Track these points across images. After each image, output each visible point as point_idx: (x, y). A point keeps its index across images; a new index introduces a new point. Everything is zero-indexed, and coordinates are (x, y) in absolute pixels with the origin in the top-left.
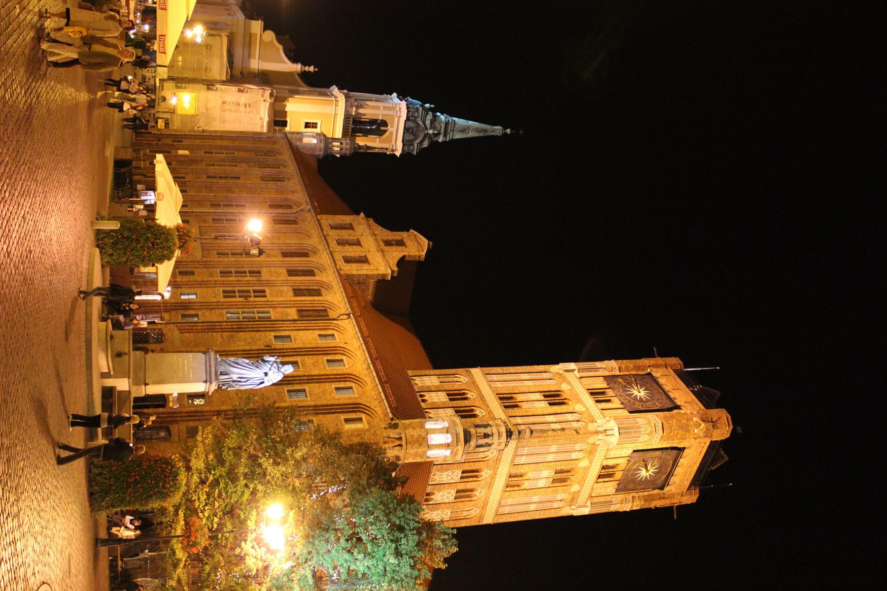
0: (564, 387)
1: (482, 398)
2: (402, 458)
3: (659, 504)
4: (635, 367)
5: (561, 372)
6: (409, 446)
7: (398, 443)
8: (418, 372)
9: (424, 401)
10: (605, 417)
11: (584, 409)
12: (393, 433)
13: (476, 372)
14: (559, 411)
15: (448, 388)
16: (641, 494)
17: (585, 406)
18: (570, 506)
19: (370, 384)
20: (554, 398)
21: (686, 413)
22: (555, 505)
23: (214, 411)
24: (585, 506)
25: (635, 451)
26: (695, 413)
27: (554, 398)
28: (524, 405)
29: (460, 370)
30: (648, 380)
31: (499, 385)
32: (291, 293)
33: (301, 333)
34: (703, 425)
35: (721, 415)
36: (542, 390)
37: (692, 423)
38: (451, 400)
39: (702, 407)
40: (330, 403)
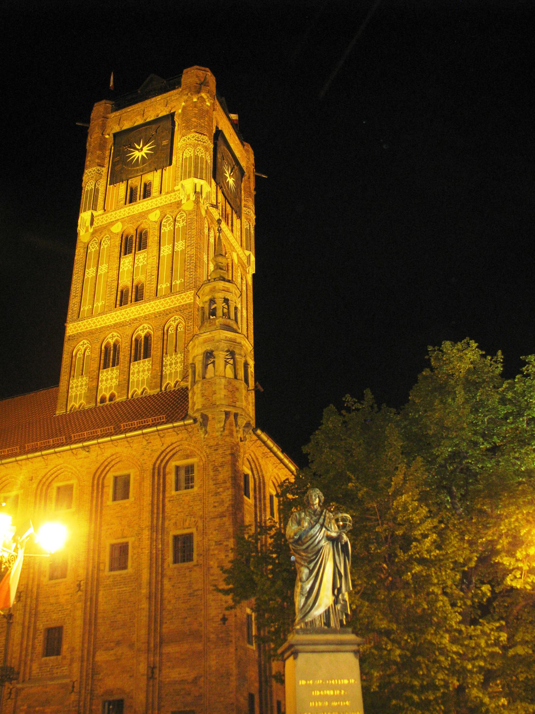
0: (117, 229)
1: (117, 326)
2: (248, 419)
3: (252, 186)
4: (100, 149)
5: (91, 230)
6: (238, 404)
7: (232, 417)
8: (61, 401)
9: (111, 399)
10: (174, 191)
11: (158, 212)
12: (217, 425)
13: (72, 328)
14: (156, 238)
15: (96, 366)
16: (243, 197)
17: (152, 210)
19: (118, 449)
20: (133, 242)
21: (184, 108)
22: (244, 288)
23: (148, 685)
24: (249, 257)
25: (214, 177)
26: (186, 97)
27: (133, 242)
28: (140, 278)
29: (67, 347)
30: (125, 139)
31: (99, 304)
34: (203, 95)
35: (192, 75)
37: (199, 105)
39: (175, 91)
40: (149, 508)
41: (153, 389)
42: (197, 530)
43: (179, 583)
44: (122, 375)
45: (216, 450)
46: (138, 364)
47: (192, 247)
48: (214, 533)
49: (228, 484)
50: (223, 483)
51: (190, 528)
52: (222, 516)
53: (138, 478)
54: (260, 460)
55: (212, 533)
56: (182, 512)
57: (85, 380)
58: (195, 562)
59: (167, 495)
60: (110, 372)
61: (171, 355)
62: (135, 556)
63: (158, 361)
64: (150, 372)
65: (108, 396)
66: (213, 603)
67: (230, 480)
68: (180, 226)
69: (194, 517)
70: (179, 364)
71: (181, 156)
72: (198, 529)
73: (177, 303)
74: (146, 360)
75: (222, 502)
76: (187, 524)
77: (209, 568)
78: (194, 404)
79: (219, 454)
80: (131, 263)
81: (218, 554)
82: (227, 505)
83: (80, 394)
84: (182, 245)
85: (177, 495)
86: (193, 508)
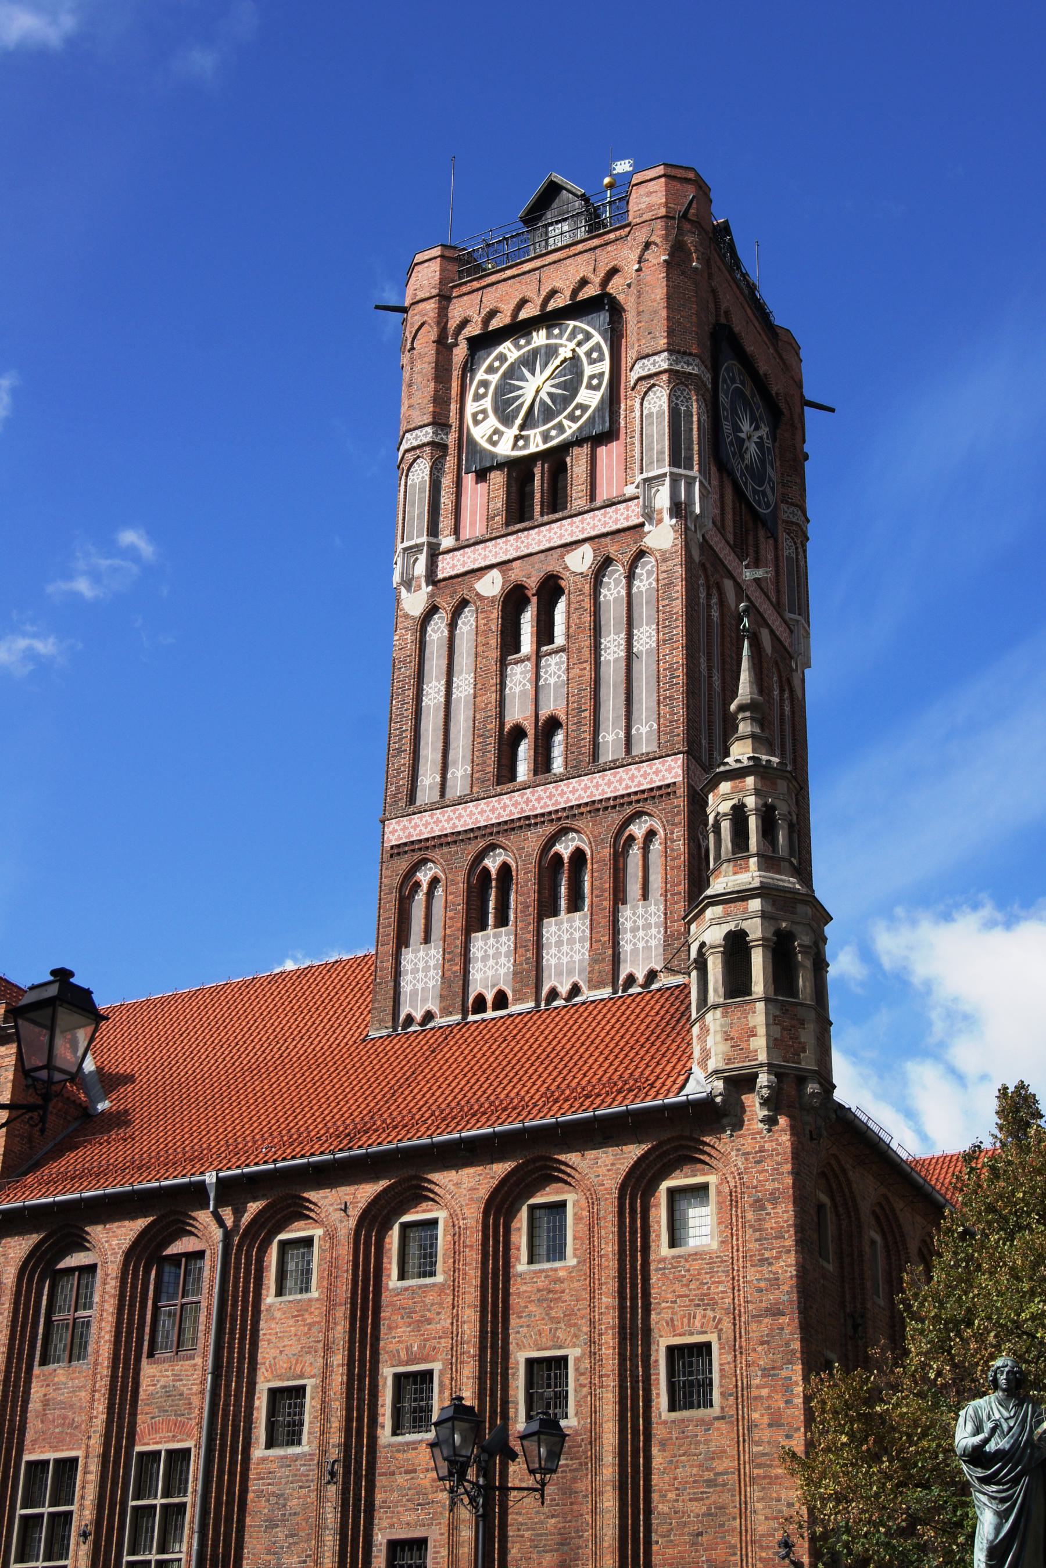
0: (491, 586)
15: (459, 923)
18: (792, 670)
32: (59, 1372)
33: (266, 1353)
36: (494, 654)
38: (502, 921)
41: (597, 987)
42: (720, 1339)
43: (684, 1455)
44: (520, 951)
45: (758, 1162)
46: (559, 924)
47: (675, 645)
48: (759, 1348)
49: (789, 1242)
50: (776, 1238)
51: (705, 1332)
52: (775, 1312)
53: (585, 1213)
54: (851, 1173)
55: (755, 1350)
56: (687, 1296)
57: (434, 953)
58: (716, 1410)
59: (652, 1257)
60: (492, 941)
61: (635, 908)
62: (586, 1390)
63: (604, 922)
64: (587, 945)
65: (490, 997)
66: (759, 1506)
67: (792, 1230)
68: (644, 589)
69: (713, 1310)
70: (654, 931)
71: (637, 406)
72: (724, 1336)
73: (645, 782)
74: (577, 915)
75: (774, 1282)
76: (697, 1323)
77: (751, 1426)
78: (706, 1057)
79: (767, 1171)
80: (529, 675)
81: (769, 1397)
82: (785, 1288)
83: (423, 989)
84: (650, 637)
85: (673, 1257)
86: (709, 1288)
